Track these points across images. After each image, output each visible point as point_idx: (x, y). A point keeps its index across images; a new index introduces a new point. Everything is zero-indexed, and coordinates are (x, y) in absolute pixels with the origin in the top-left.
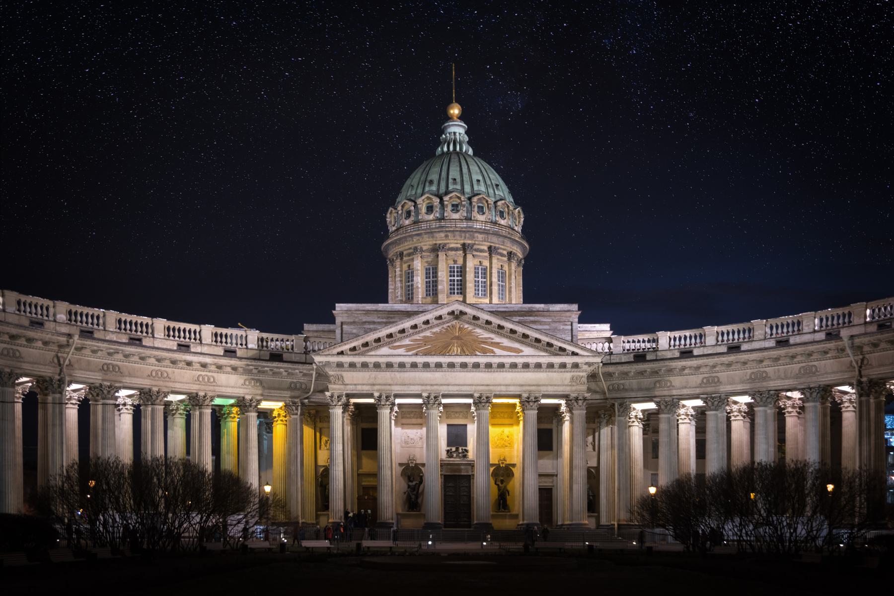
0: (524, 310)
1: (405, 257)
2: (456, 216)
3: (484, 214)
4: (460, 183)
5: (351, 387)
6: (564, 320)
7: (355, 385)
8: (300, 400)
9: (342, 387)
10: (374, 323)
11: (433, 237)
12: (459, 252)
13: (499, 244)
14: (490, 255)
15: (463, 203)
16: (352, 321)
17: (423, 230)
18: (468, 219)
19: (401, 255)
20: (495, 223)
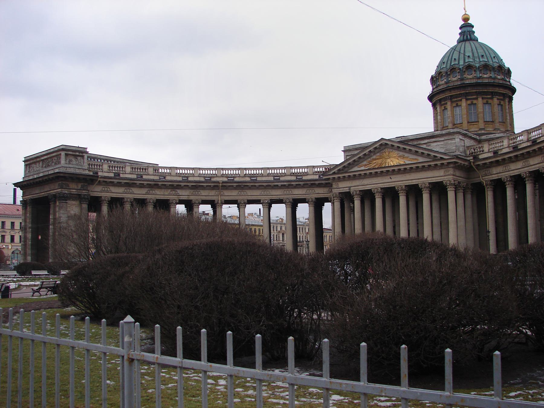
5: (341, 189)
7: (343, 188)
12: (458, 99)
15: (458, 71)
18: (462, 79)
20: (480, 78)
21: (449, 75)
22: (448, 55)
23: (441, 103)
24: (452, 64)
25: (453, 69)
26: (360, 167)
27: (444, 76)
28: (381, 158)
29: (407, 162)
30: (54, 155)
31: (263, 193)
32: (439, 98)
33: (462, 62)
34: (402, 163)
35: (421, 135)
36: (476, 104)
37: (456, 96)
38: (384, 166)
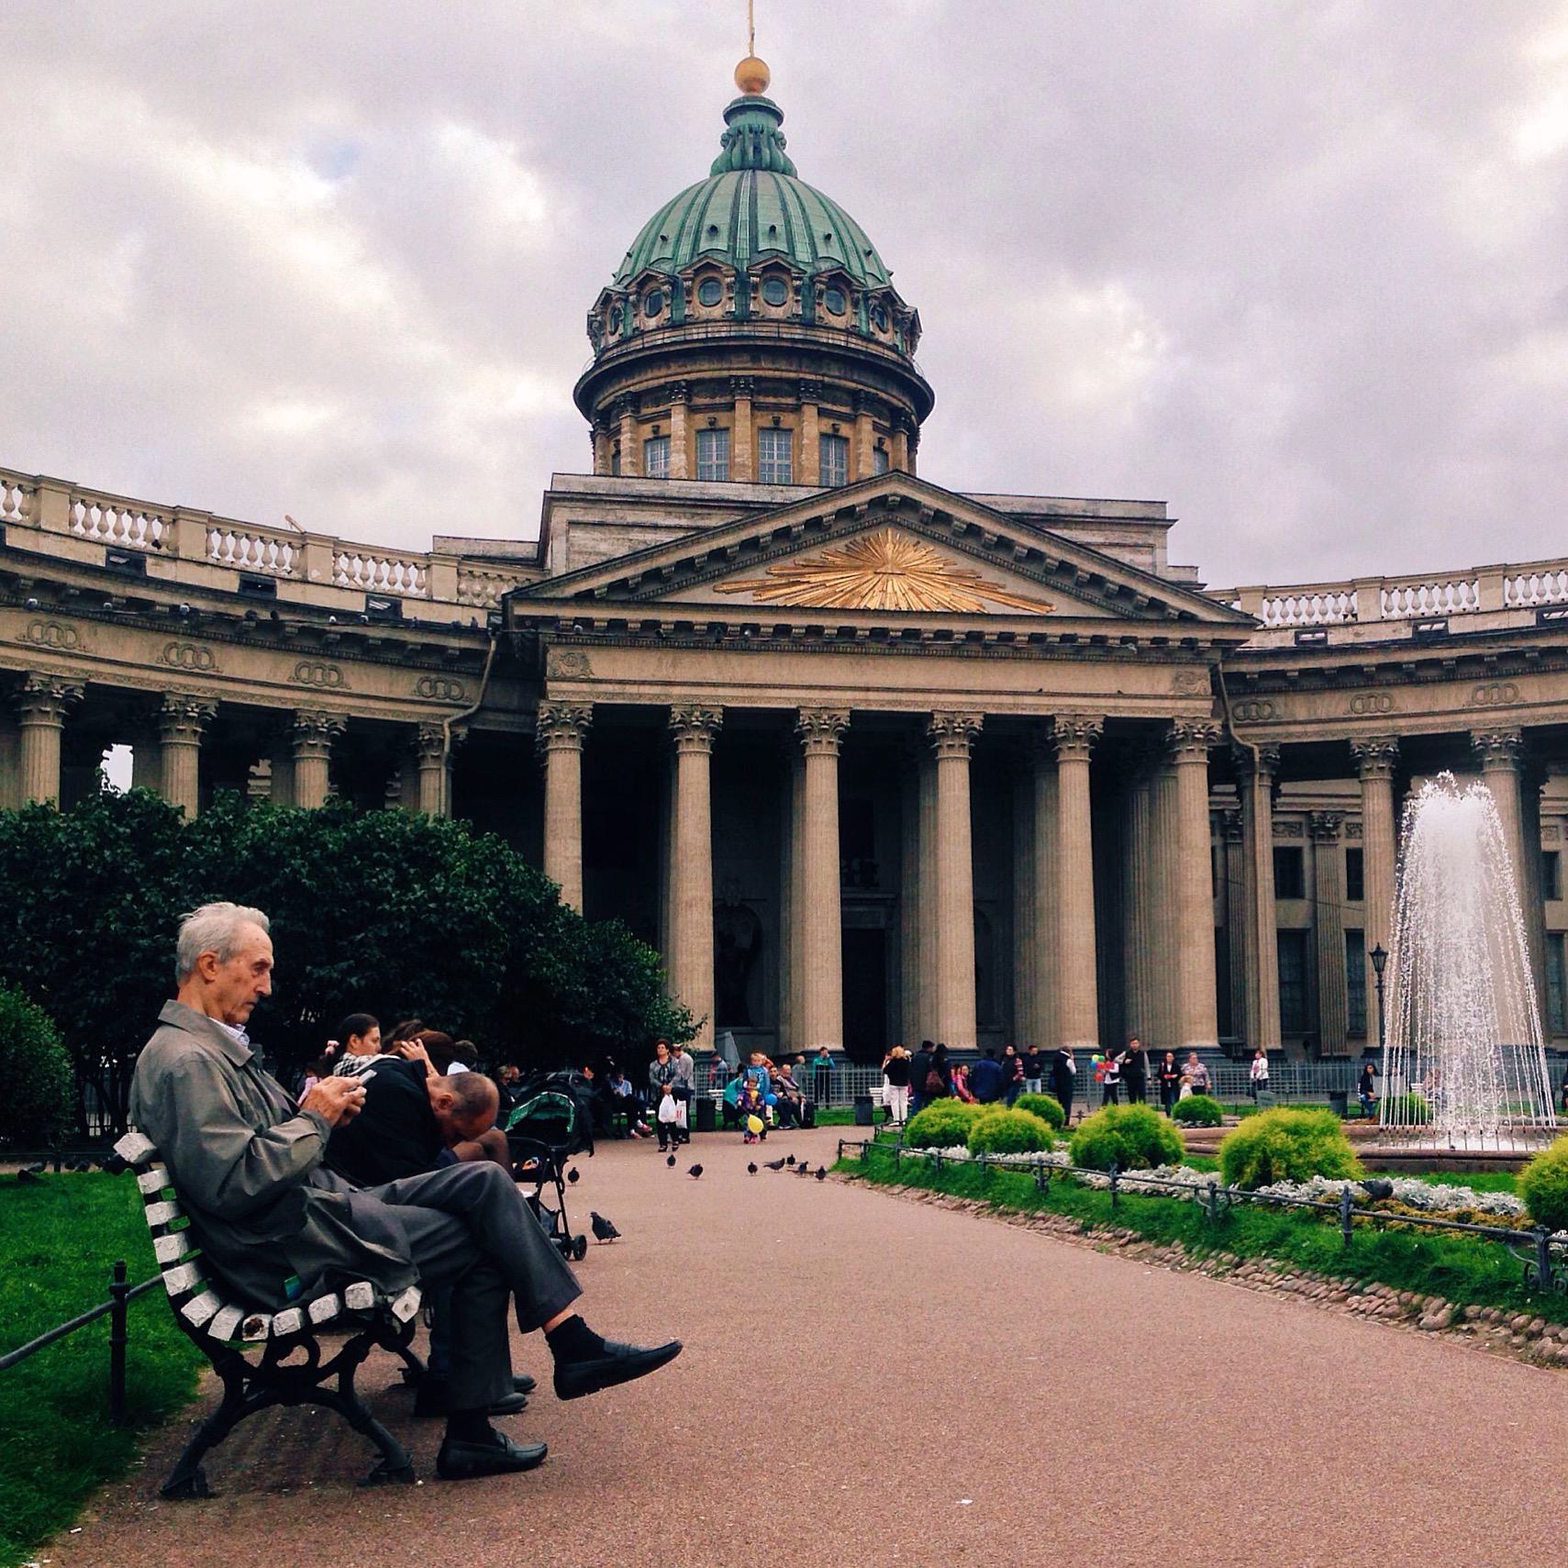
0: (1037, 511)
3: (844, 314)
4: (784, 236)
5: (610, 688)
6: (1134, 540)
9: (585, 687)
10: (656, 527)
11: (721, 360)
12: (783, 400)
13: (876, 389)
14: (855, 409)
15: (798, 283)
16: (597, 520)
17: (698, 340)
19: (636, 400)
20: (869, 338)
21: (755, 287)
22: (722, 201)
23: (689, 399)
24: (763, 246)
25: (777, 267)
26: (728, 592)
27: (729, 287)
28: (857, 568)
29: (993, 608)
32: (686, 377)
33: (803, 254)
34: (967, 602)
36: (846, 440)
37: (776, 387)
38: (873, 604)
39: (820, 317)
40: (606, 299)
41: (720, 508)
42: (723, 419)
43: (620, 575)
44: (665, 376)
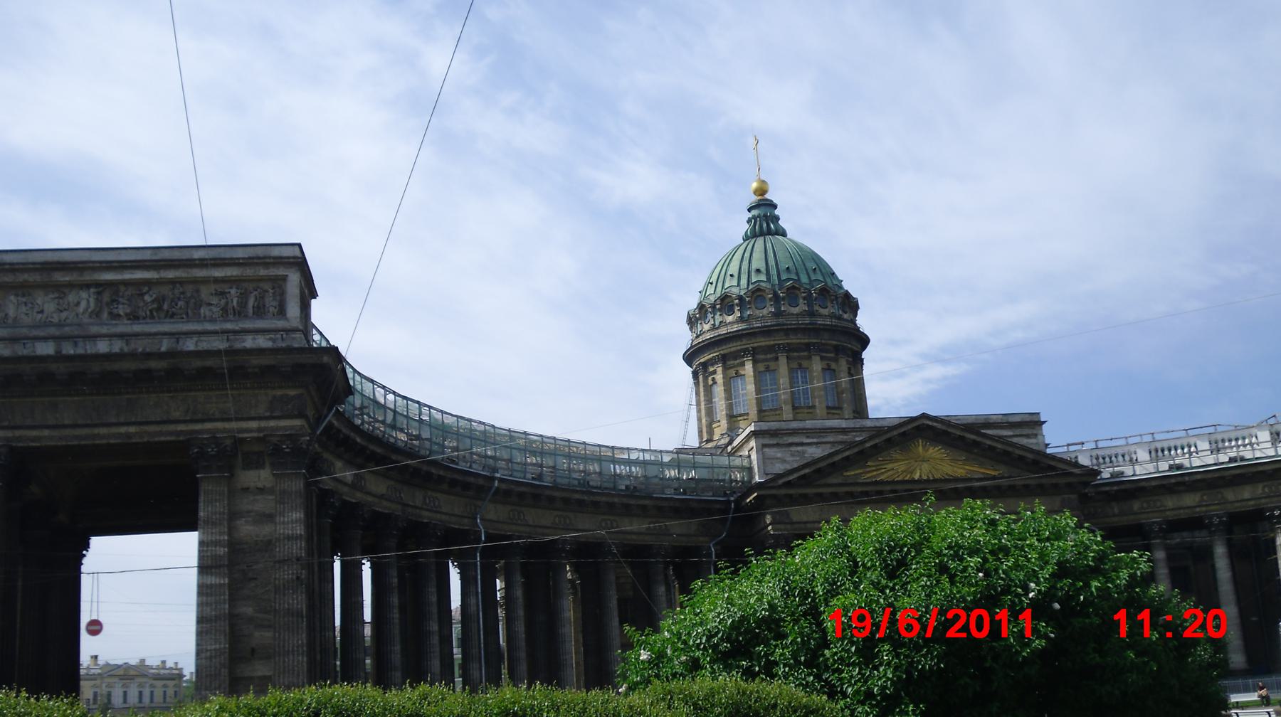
0: (980, 422)
1: (729, 360)
2: (796, 310)
3: (826, 308)
7: (806, 523)
8: (713, 545)
9: (789, 526)
10: (802, 444)
12: (802, 354)
14: (837, 354)
15: (805, 294)
16: (775, 442)
17: (758, 327)
18: (812, 314)
20: (840, 318)
24: (784, 277)
25: (793, 287)
27: (770, 299)
28: (907, 460)
30: (218, 273)
31: (557, 520)
32: (752, 345)
33: (804, 279)
34: (960, 471)
35: (959, 419)
36: (834, 370)
38: (917, 477)
39: (817, 311)
40: (701, 307)
41: (831, 432)
42: (772, 365)
43: (802, 472)
44: (740, 345)
